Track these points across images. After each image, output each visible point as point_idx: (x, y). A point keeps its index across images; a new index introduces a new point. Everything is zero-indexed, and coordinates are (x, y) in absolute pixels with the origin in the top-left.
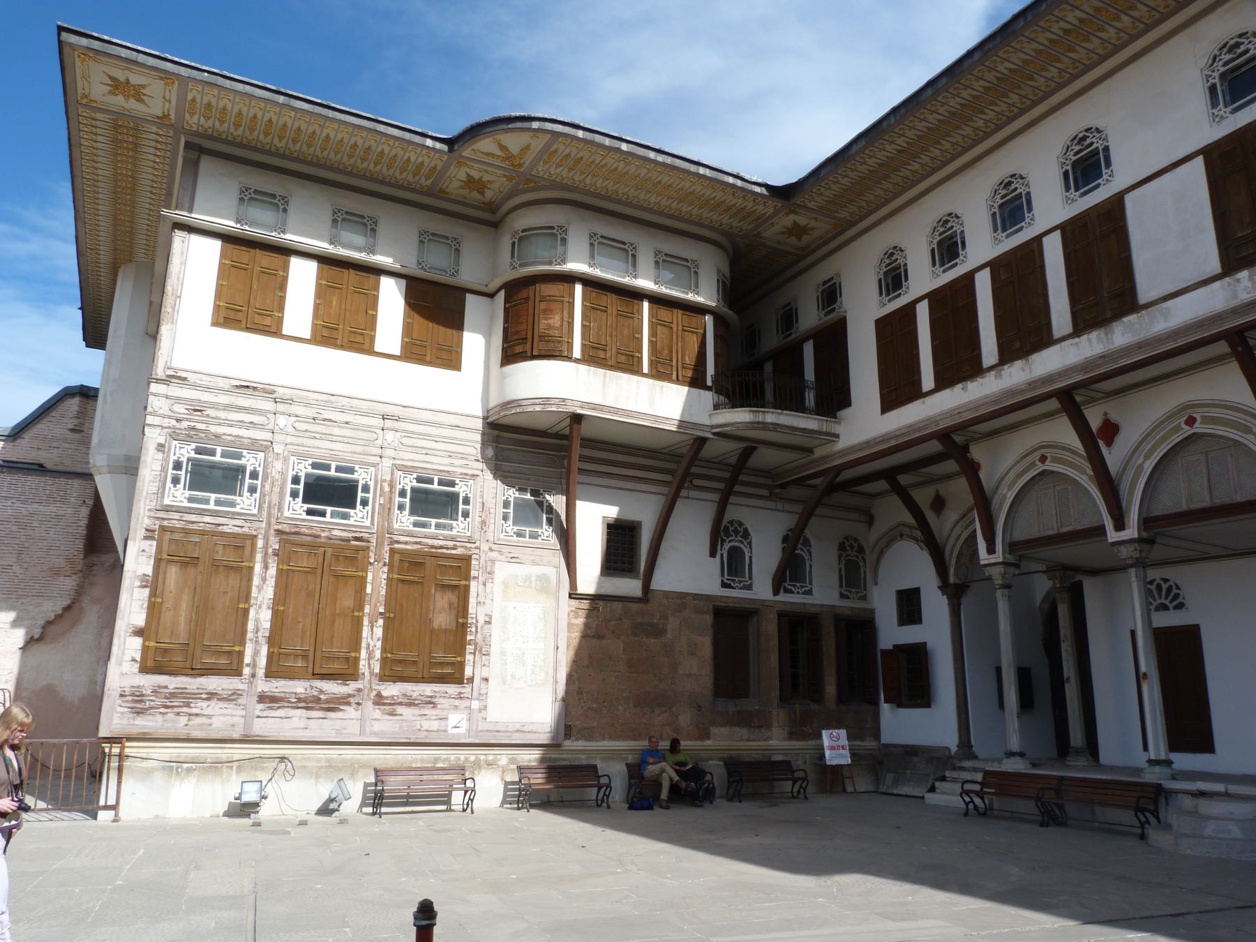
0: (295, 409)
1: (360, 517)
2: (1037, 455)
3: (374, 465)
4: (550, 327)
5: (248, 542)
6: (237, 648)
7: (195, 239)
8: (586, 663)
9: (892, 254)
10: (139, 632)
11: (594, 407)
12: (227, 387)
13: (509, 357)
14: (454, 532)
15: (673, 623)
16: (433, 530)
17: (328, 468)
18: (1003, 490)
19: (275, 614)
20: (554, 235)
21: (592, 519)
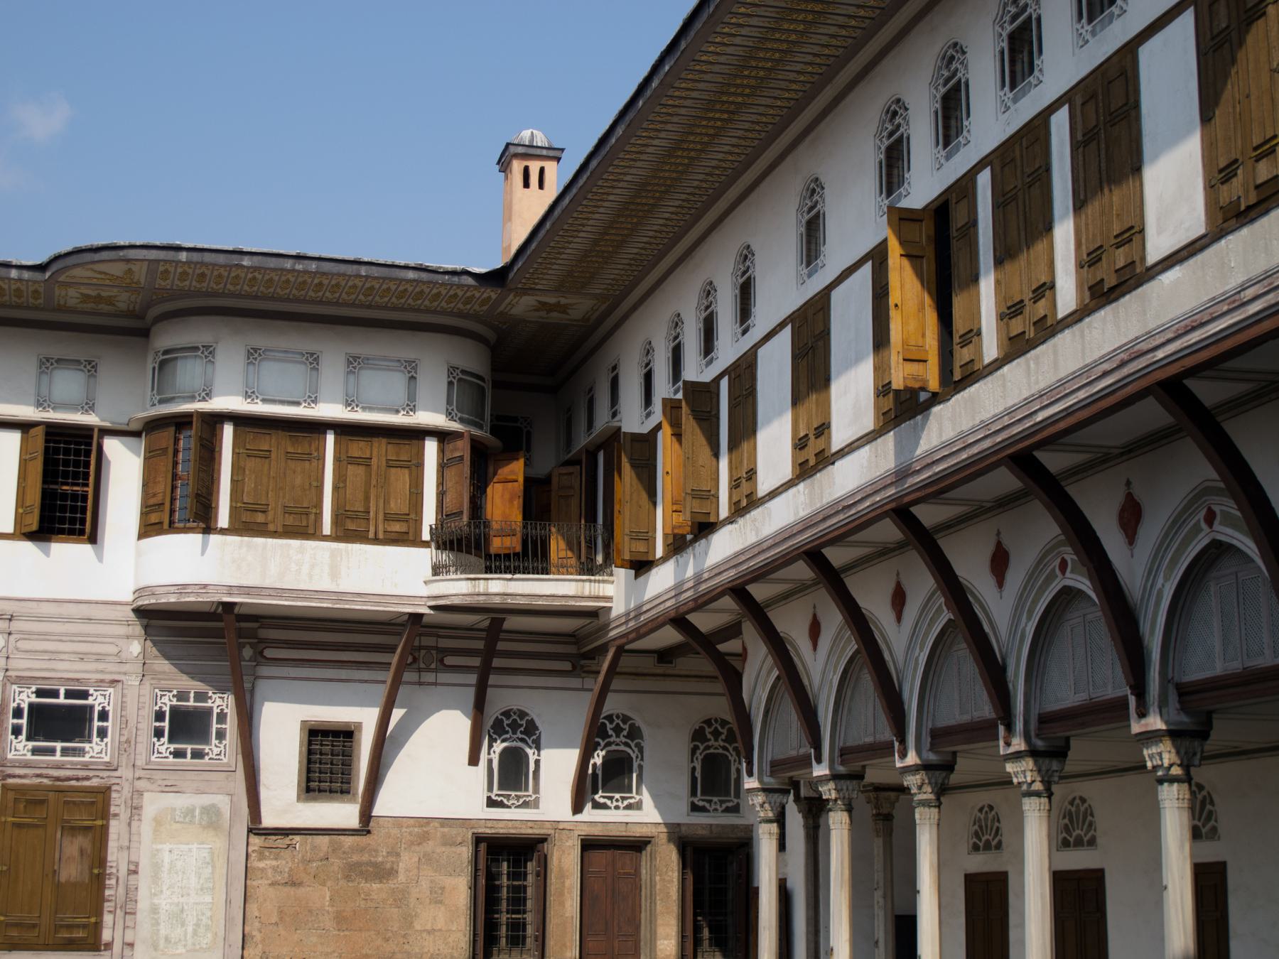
8: (274, 919)
11: (247, 590)
13: (149, 528)
14: (87, 758)
15: (407, 861)
16: (58, 757)
21: (282, 726)
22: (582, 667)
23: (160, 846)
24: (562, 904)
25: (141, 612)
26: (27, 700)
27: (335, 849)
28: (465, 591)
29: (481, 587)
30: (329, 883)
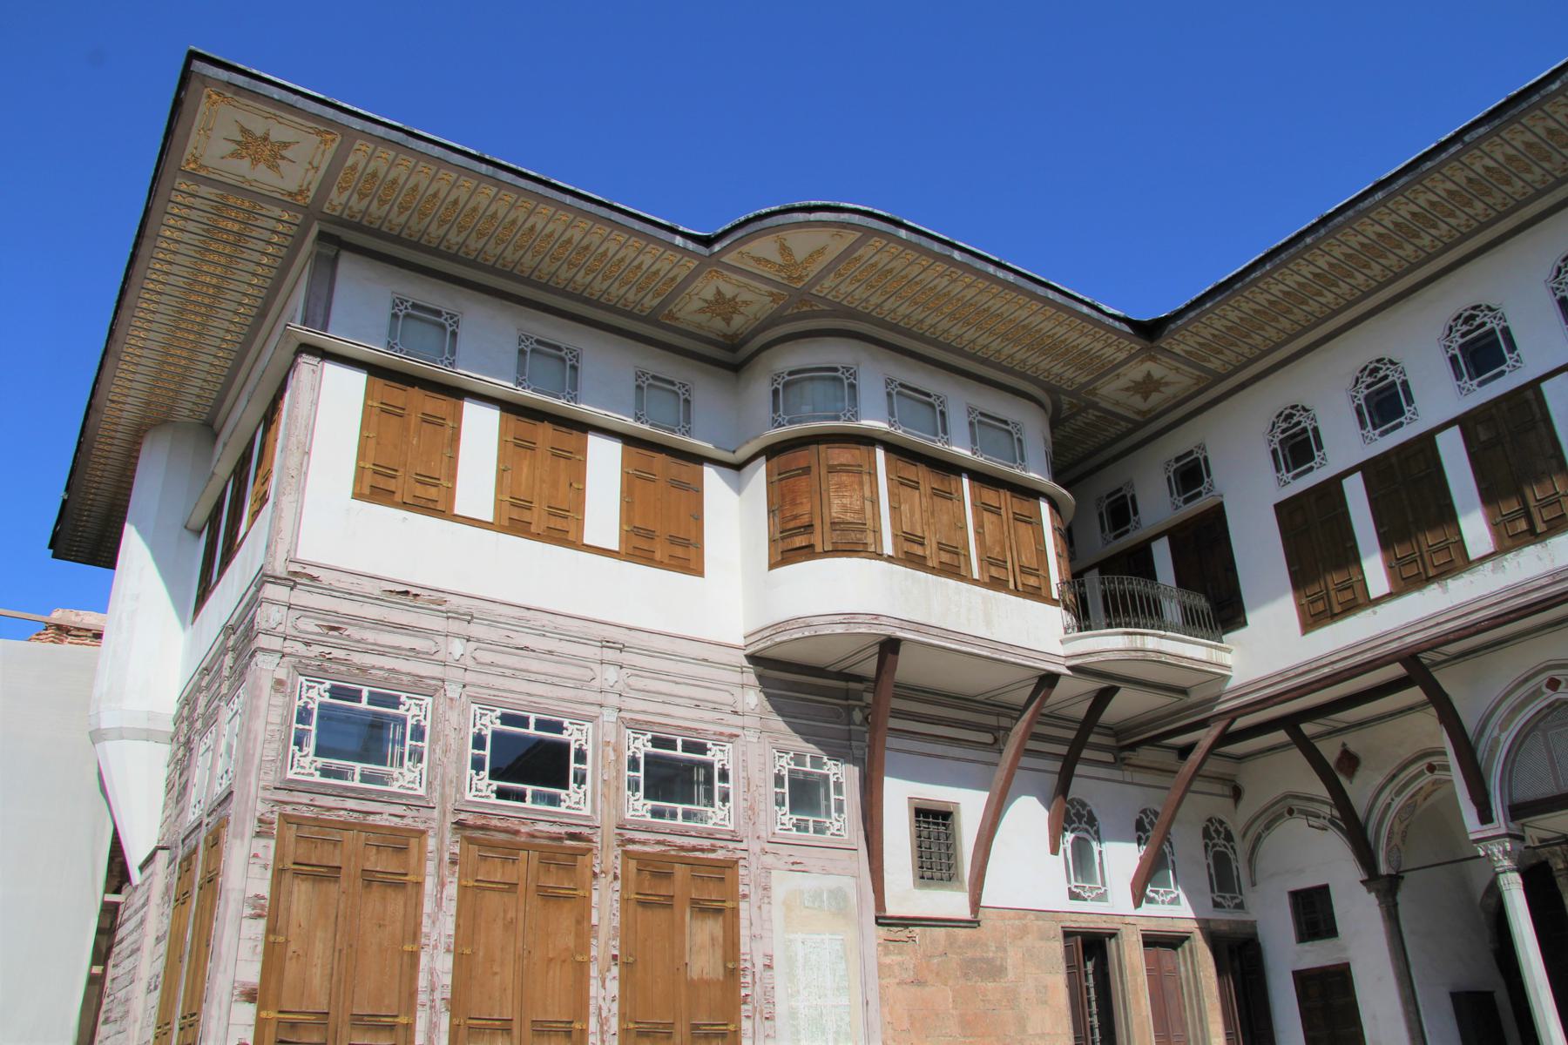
0: (476, 630)
1: (575, 801)
2: (1543, 678)
3: (591, 719)
4: (845, 509)
5: (414, 842)
6: (403, 1020)
7: (331, 370)
8: (906, 1025)
9: (1290, 416)
10: (250, 996)
12: (377, 593)
14: (710, 825)
15: (1013, 957)
16: (679, 820)
17: (524, 722)
18: (1492, 730)
19: (459, 959)
20: (841, 380)
22: (1123, 759)
23: (792, 936)
24: (1138, 1002)
25: (754, 659)
26: (643, 750)
27: (952, 942)
28: (1121, 646)
29: (1138, 642)
30: (951, 983)
